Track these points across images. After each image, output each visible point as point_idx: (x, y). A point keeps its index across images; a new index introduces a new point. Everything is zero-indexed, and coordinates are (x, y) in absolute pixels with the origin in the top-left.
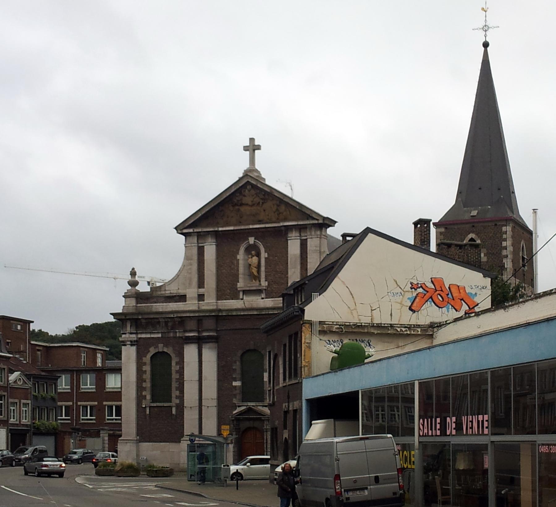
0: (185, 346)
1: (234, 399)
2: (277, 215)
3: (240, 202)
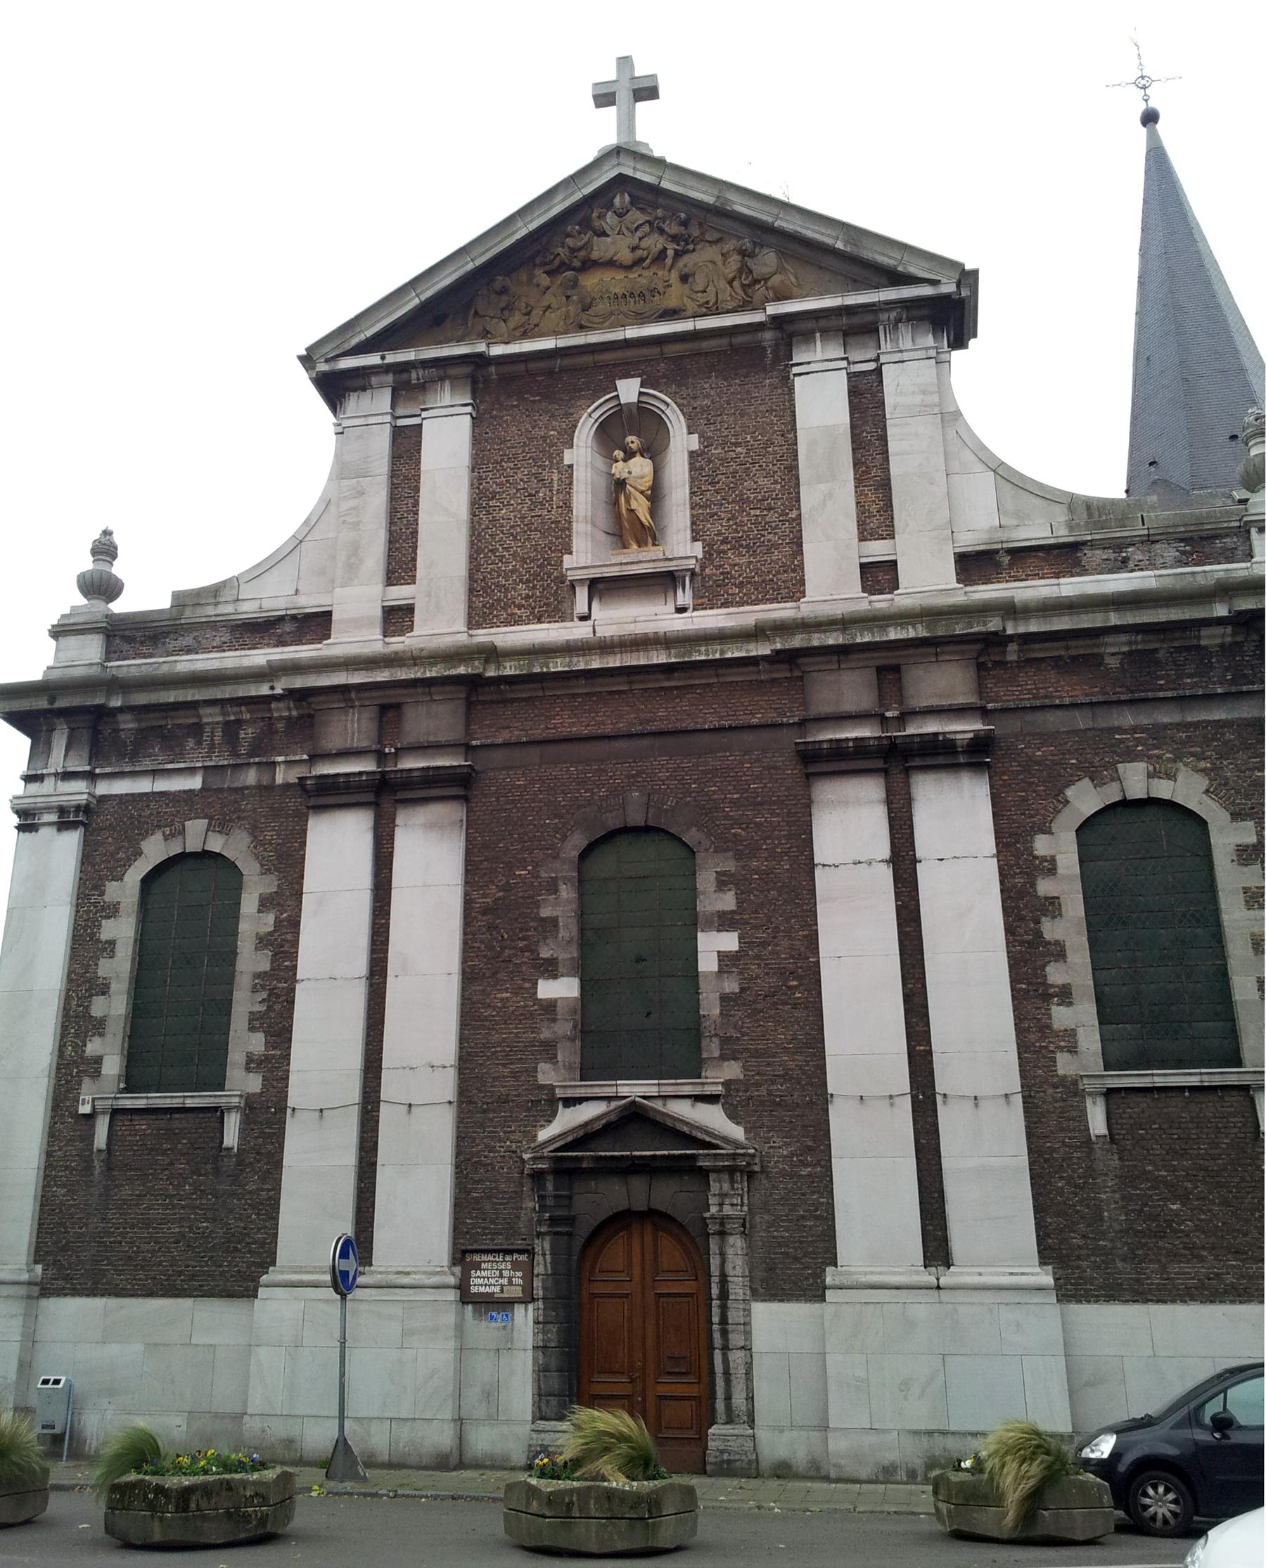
0: (312, 823)
1: (543, 1066)
2: (740, 291)
3: (582, 253)
